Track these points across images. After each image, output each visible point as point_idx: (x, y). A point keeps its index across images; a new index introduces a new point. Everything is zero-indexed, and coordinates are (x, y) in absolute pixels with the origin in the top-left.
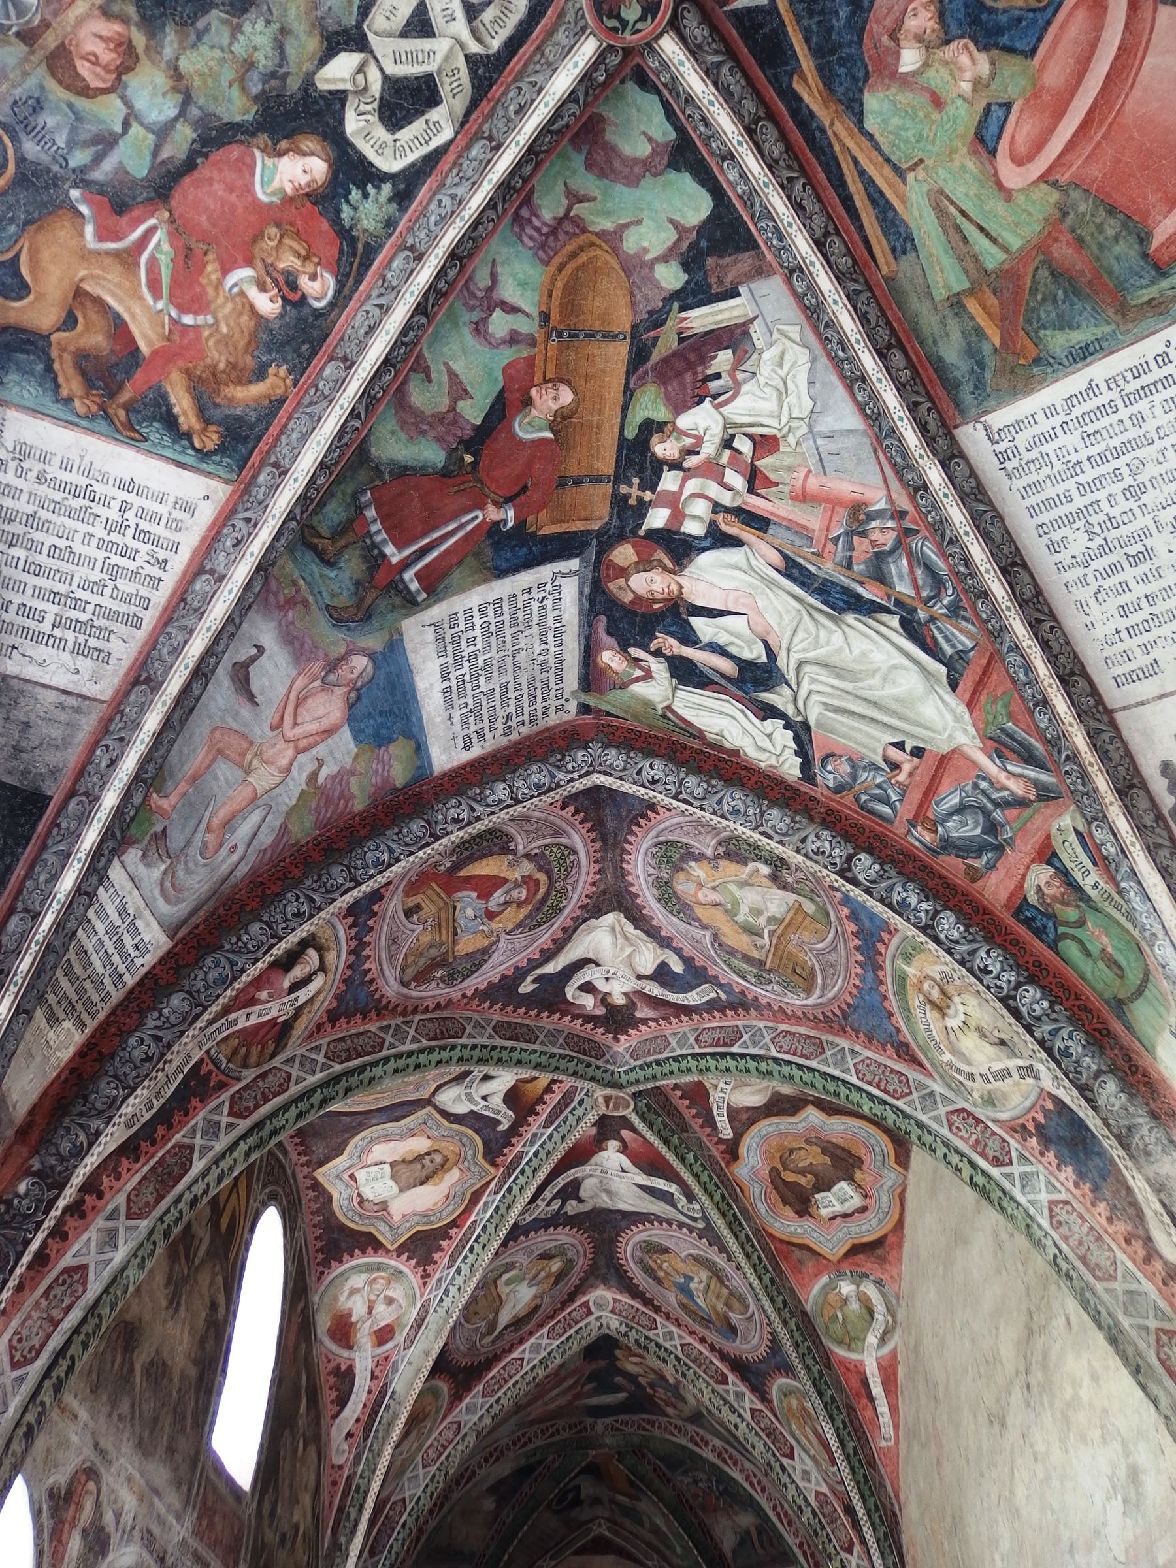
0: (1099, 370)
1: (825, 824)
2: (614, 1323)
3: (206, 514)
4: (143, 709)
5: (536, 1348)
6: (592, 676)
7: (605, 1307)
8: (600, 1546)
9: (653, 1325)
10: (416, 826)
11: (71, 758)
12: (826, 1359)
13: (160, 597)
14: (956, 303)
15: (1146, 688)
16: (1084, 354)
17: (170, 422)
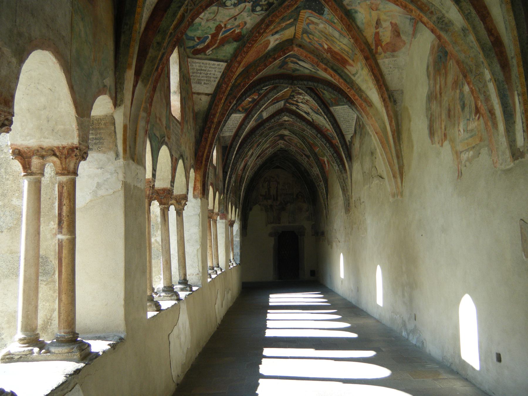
0: (345, 106)
1: (315, 129)
2: (283, 146)
3: (243, 117)
4: (239, 140)
5: (269, 151)
6: (285, 105)
7: (281, 144)
8: (277, 167)
9: (290, 147)
10: (262, 127)
11: (230, 142)
12: (318, 159)
13: (238, 125)
14: (330, 99)
15: (348, 133)
16: (343, 105)
17: (239, 111)
